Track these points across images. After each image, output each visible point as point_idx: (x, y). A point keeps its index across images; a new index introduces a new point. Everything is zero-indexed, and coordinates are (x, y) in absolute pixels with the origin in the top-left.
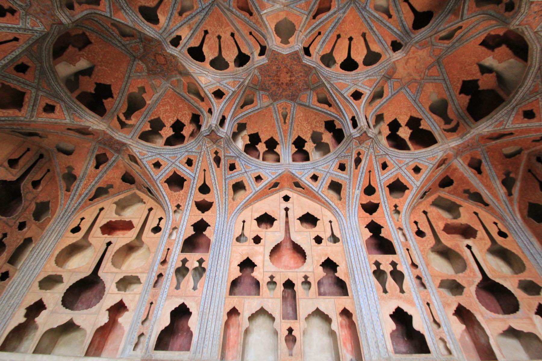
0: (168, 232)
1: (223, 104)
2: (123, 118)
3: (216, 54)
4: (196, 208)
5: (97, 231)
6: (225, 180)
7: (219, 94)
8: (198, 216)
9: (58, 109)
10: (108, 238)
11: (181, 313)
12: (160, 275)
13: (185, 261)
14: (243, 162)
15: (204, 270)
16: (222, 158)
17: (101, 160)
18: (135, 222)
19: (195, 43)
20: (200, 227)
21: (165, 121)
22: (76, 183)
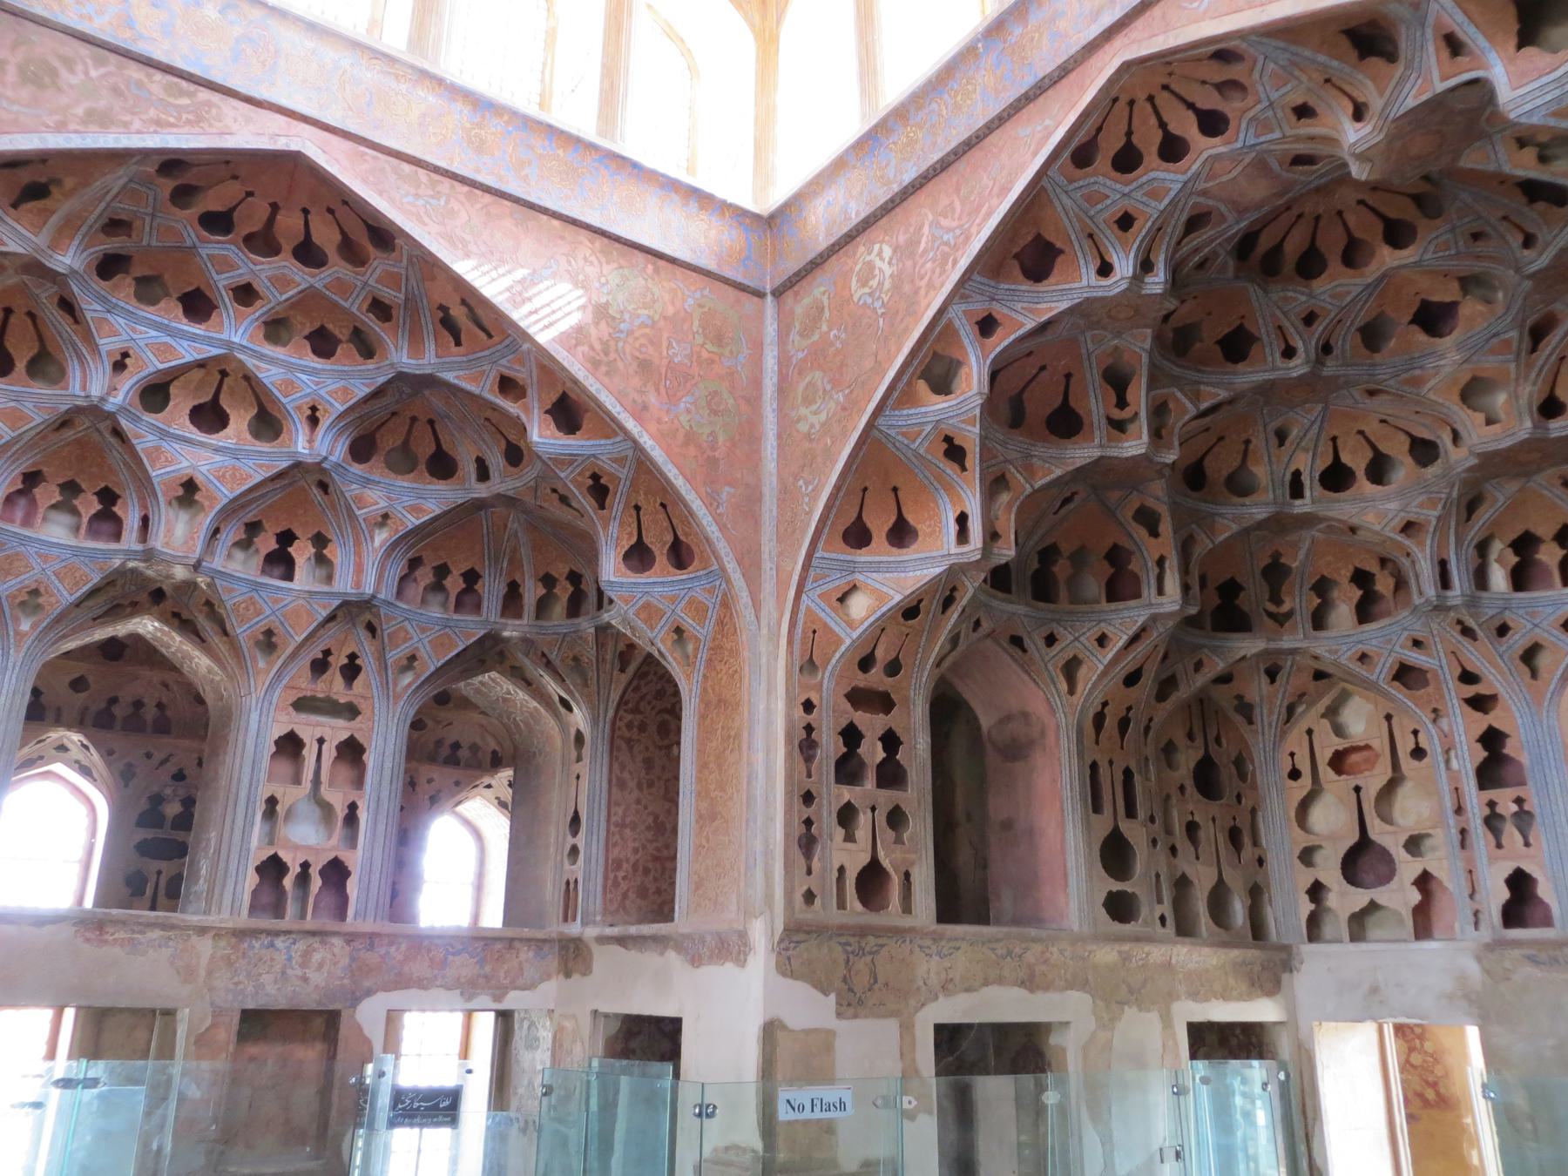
0: (1440, 759)
1: (1428, 542)
2: (1272, 608)
3: (1370, 454)
4: (1468, 710)
5: (1326, 773)
6: (1501, 656)
7: (1408, 527)
8: (1481, 722)
9: (1205, 660)
10: (1348, 782)
11: (1520, 883)
12: (1463, 832)
13: (1492, 804)
14: (1521, 612)
15: (1529, 813)
16: (1475, 627)
17: (1272, 674)
18: (1375, 744)
19: (1325, 462)
20: (1492, 740)
21: (1334, 576)
22: (1257, 711)
